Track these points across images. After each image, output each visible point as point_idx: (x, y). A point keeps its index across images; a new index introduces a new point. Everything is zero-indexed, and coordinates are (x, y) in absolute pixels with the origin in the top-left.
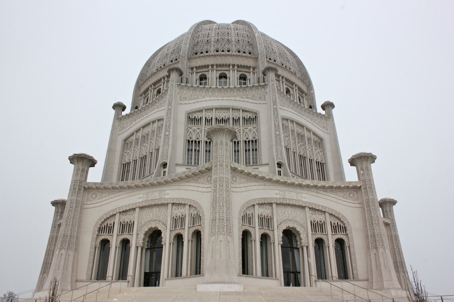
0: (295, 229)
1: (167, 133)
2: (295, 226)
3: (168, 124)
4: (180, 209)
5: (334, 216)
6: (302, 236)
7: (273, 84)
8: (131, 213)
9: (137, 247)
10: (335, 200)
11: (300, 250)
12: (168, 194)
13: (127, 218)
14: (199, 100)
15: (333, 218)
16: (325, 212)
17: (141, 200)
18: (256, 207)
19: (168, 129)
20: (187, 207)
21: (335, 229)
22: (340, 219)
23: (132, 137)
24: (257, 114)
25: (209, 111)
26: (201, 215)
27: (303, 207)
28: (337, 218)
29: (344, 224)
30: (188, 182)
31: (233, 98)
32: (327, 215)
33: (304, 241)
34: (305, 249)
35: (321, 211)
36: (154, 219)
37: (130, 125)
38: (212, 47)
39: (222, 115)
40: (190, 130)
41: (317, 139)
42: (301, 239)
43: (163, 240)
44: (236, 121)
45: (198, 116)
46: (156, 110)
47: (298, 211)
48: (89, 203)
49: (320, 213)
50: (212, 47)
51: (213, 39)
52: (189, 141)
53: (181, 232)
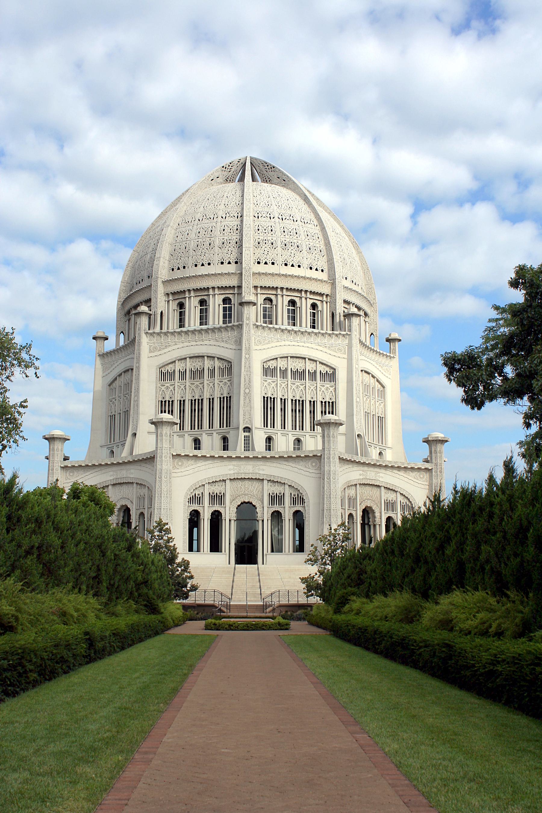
0: (370, 508)
1: (247, 391)
2: (372, 505)
4: (276, 486)
5: (404, 495)
6: (377, 514)
7: (356, 335)
8: (220, 484)
9: (230, 520)
10: (406, 479)
11: (372, 527)
13: (217, 489)
14: (274, 345)
15: (403, 497)
16: (396, 492)
17: (232, 472)
18: (346, 489)
20: (287, 487)
21: (403, 508)
22: (409, 499)
23: (170, 366)
24: (335, 369)
25: (283, 359)
26: (304, 498)
27: (378, 486)
28: (407, 498)
29: (412, 504)
30: (287, 461)
31: (309, 345)
32: (398, 494)
33: (378, 519)
34: (378, 527)
35: (394, 490)
36: (246, 492)
37: (166, 347)
38: (279, 255)
39: (299, 365)
40: (266, 384)
41: (380, 386)
42: (375, 517)
43: (258, 515)
44: (313, 376)
45: (272, 364)
46: (212, 342)
47: (375, 490)
48: (175, 471)
49: (392, 492)
50: (279, 255)
51: (279, 243)
52: (264, 397)
53: (281, 510)
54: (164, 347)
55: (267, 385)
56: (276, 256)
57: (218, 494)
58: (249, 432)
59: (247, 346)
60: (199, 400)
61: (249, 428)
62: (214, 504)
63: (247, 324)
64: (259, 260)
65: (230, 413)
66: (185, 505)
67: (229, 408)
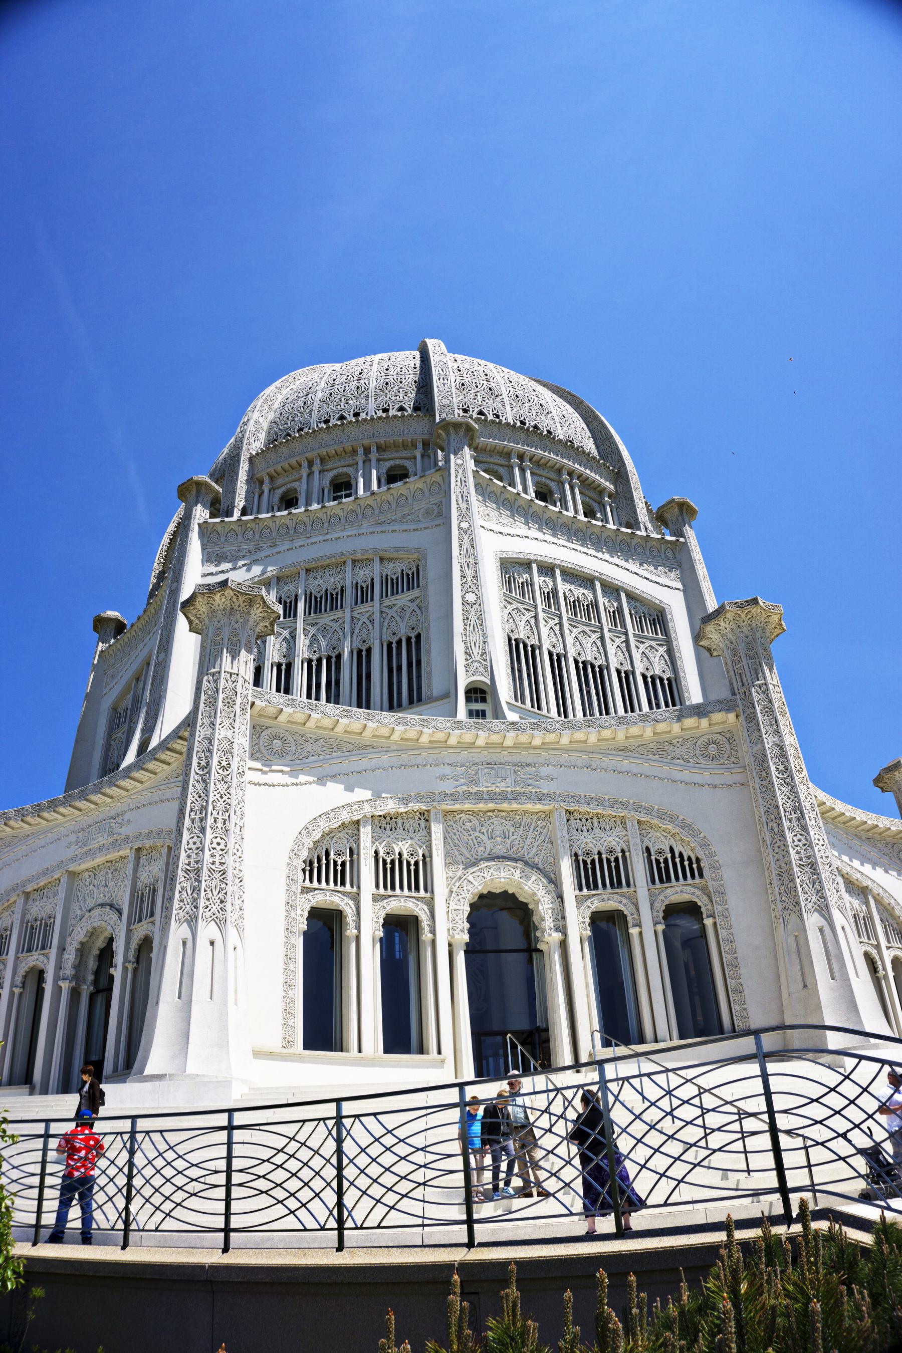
1: (471, 598)
3: (469, 573)
12: (550, 778)
19: (473, 586)
38: (508, 407)
52: (510, 639)
54: (242, 554)
55: (514, 613)
56: (500, 405)
57: (405, 856)
58: (484, 700)
59: (463, 506)
60: (329, 659)
61: (483, 692)
62: (393, 888)
63: (460, 466)
64: (465, 407)
65: (419, 676)
66: (291, 879)
67: (416, 665)
